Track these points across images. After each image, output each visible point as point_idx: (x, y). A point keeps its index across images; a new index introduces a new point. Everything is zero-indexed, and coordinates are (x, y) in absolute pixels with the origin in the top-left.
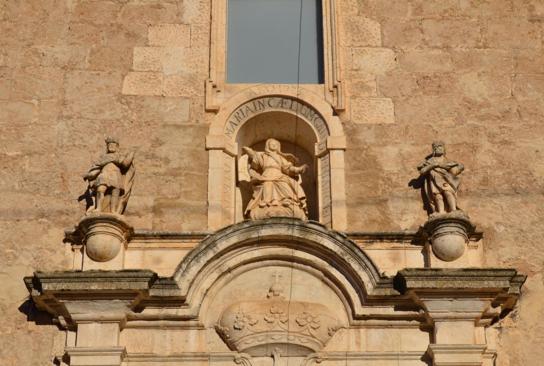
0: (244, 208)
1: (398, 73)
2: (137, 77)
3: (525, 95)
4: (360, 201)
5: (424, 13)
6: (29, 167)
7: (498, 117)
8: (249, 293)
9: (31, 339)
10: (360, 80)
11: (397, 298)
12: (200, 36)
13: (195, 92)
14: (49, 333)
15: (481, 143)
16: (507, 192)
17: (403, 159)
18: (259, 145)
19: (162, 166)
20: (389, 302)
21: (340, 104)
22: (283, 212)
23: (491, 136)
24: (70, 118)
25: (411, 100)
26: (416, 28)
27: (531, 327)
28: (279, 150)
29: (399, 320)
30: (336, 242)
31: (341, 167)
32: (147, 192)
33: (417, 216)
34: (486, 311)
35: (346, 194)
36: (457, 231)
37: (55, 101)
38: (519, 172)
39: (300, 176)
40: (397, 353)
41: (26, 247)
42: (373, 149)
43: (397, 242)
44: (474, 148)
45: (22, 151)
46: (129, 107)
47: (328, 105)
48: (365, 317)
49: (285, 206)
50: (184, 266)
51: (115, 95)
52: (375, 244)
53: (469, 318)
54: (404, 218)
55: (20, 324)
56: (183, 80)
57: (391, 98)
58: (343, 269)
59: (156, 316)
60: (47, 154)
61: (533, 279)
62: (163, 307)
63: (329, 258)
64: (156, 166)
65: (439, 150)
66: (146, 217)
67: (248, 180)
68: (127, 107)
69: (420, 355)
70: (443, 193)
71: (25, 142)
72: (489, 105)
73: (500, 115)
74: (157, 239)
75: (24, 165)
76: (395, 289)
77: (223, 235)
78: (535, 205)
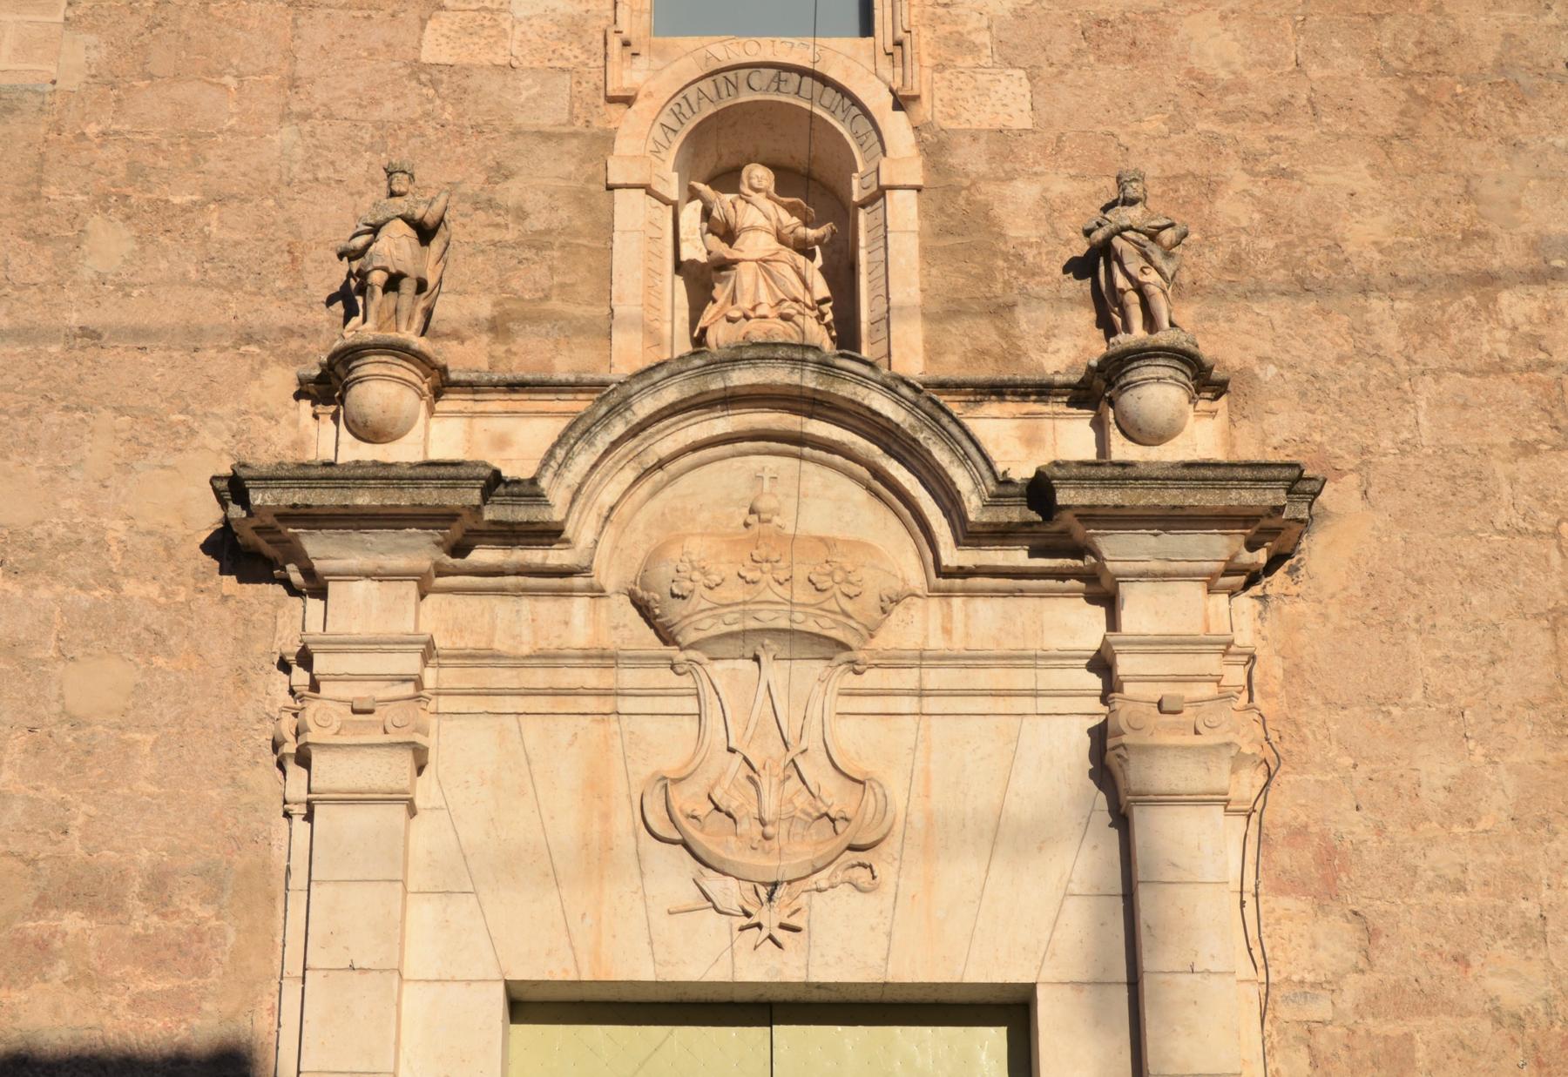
0: (693, 322)
1: (1042, 13)
3: (1325, 64)
4: (954, 306)
7: (1265, 115)
8: (704, 516)
10: (955, 28)
11: (1036, 528)
15: (1227, 174)
16: (1284, 287)
17: (1051, 210)
18: (727, 179)
20: (1016, 538)
21: (909, 84)
22: (780, 331)
23: (1250, 159)
25: (1070, 75)
27: (1333, 596)
28: (772, 189)
29: (1039, 579)
30: (899, 400)
31: (911, 227)
33: (1081, 342)
34: (1232, 558)
35: (922, 291)
36: (1171, 377)
38: (1310, 242)
39: (817, 248)
40: (1033, 653)
42: (984, 187)
43: (1035, 401)
44: (1211, 187)
47: (883, 85)
48: (963, 573)
49: (785, 318)
50: (560, 453)
52: (986, 405)
53: (1195, 575)
54: (1052, 346)
57: (1024, 69)
58: (915, 463)
61: (1340, 486)
62: (513, 545)
63: (884, 438)
65: (1133, 190)
67: (702, 258)
69: (1086, 658)
70: (1140, 289)
72: (1244, 88)
73: (1269, 110)
76: (1031, 507)
77: (646, 382)
78: (1346, 318)
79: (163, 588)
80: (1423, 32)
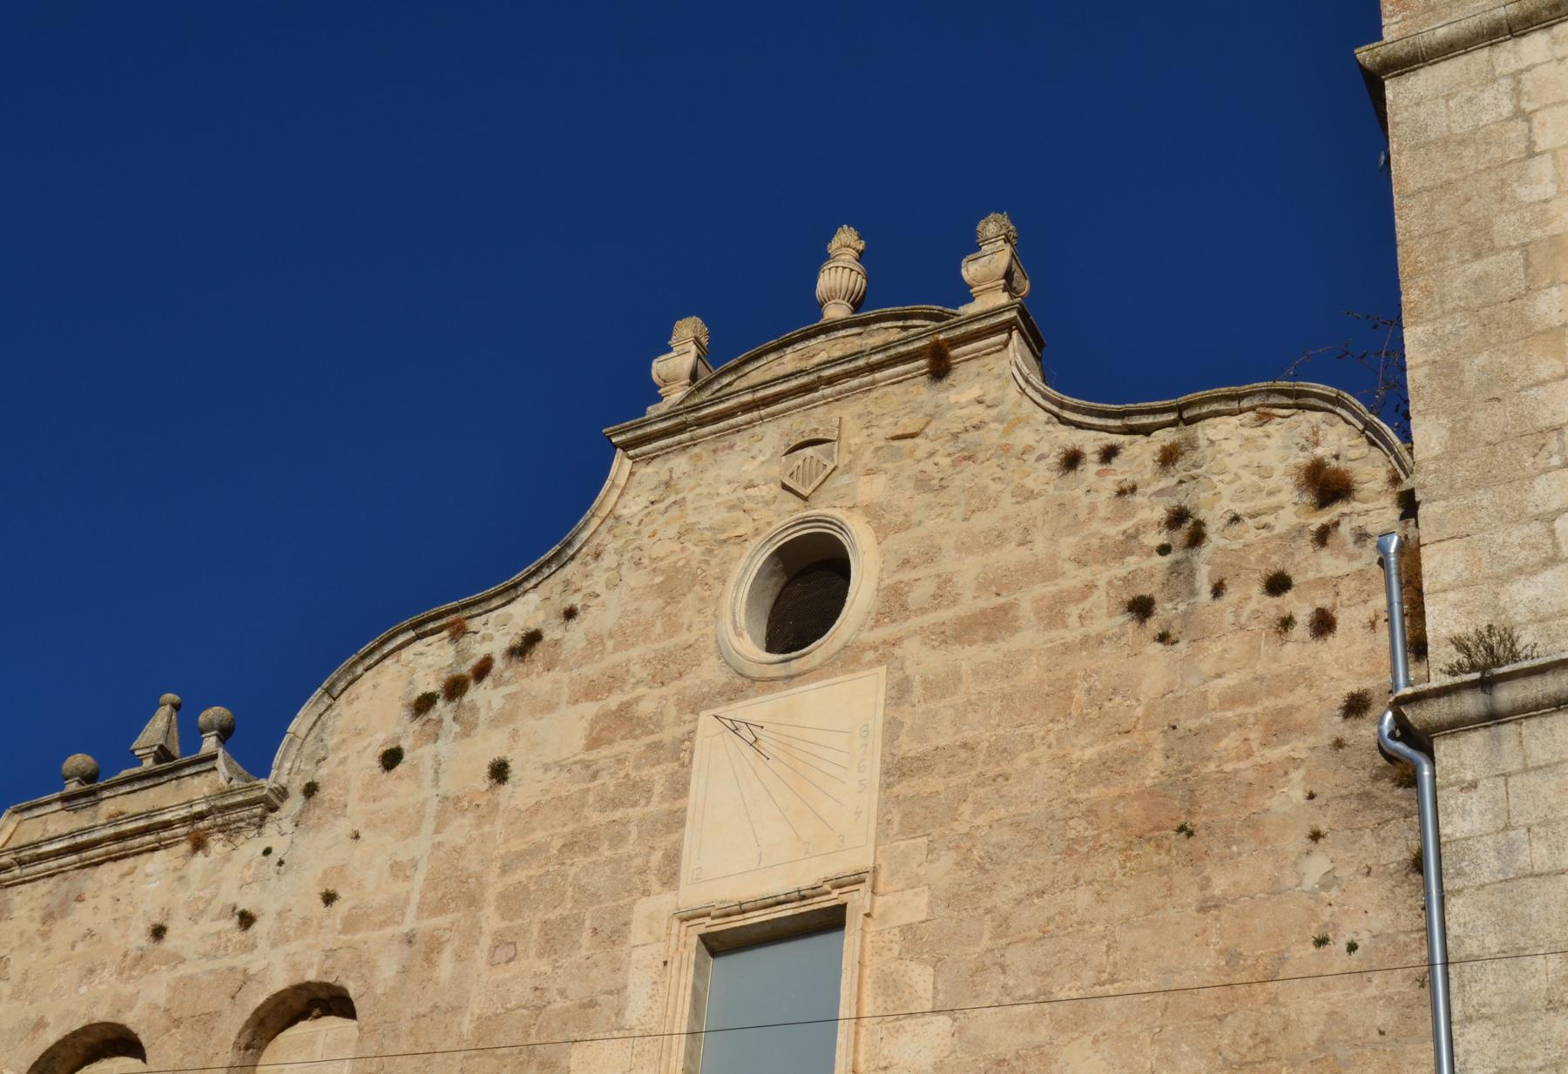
5: (1012, 931)
12: (646, 1048)
26: (994, 964)
80: (1259, 1024)
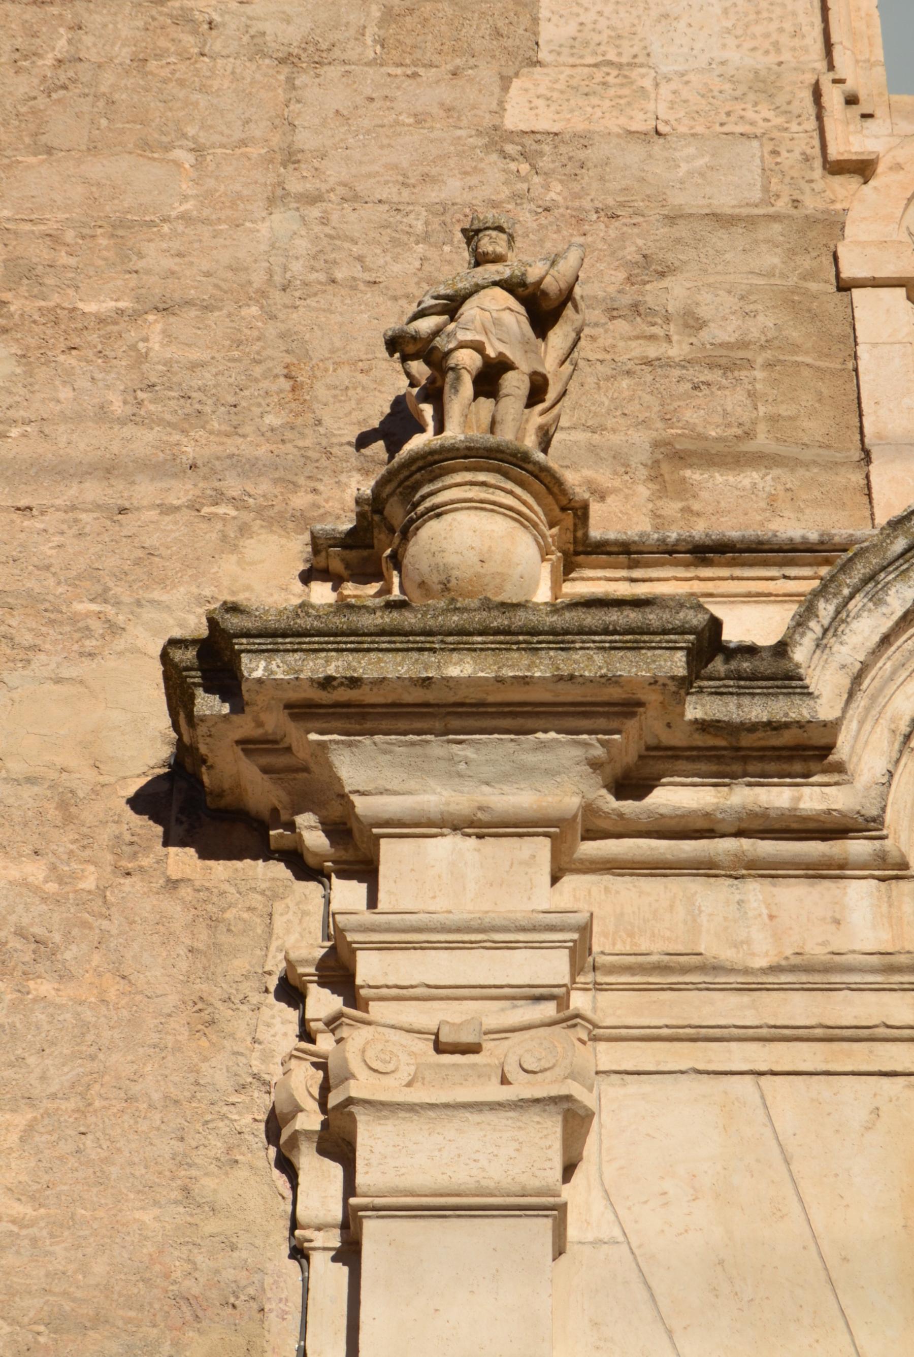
2: (556, 81)
6: (162, 345)
9: (179, 908)
13: (780, 121)
14: (253, 889)
19: (675, 338)
24: (314, 199)
32: (622, 421)
37: (255, 151)
41: (156, 595)
45: (138, 299)
46: (533, 166)
51: (479, 133)
55: (134, 856)
56: (727, 87)
59: (707, 815)
60: (230, 307)
62: (734, 776)
64: (652, 337)
66: (626, 497)
68: (525, 168)
71: (148, 272)
74: (677, 564)
75: (146, 340)
79: (53, 868)
